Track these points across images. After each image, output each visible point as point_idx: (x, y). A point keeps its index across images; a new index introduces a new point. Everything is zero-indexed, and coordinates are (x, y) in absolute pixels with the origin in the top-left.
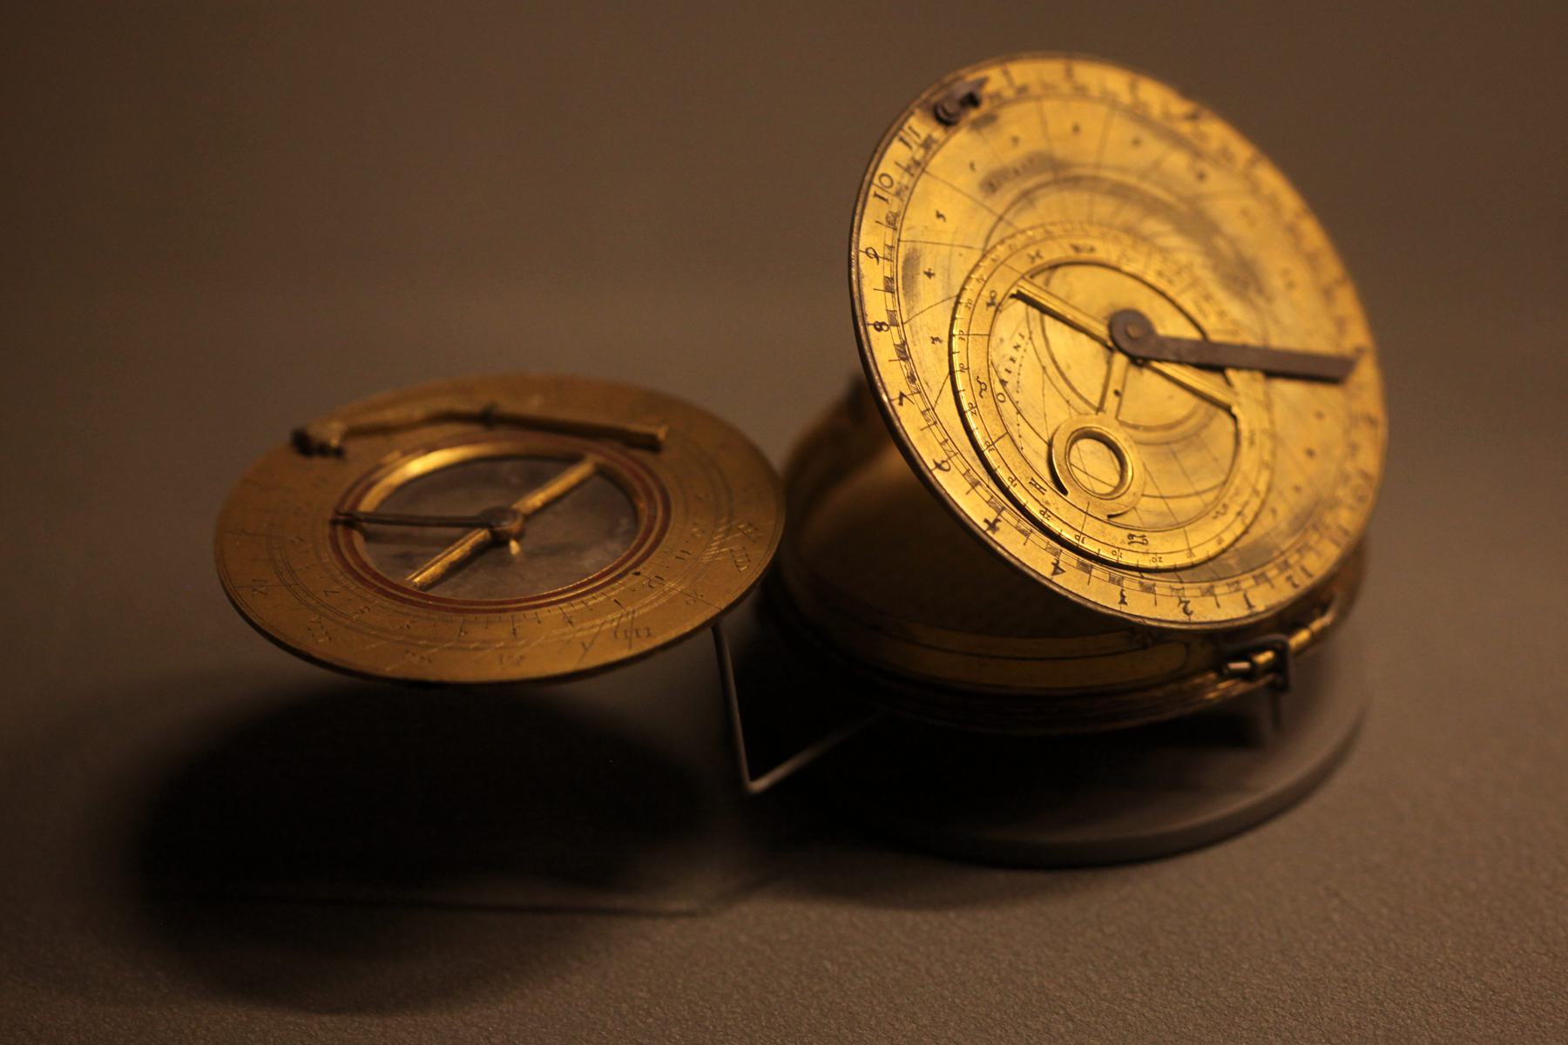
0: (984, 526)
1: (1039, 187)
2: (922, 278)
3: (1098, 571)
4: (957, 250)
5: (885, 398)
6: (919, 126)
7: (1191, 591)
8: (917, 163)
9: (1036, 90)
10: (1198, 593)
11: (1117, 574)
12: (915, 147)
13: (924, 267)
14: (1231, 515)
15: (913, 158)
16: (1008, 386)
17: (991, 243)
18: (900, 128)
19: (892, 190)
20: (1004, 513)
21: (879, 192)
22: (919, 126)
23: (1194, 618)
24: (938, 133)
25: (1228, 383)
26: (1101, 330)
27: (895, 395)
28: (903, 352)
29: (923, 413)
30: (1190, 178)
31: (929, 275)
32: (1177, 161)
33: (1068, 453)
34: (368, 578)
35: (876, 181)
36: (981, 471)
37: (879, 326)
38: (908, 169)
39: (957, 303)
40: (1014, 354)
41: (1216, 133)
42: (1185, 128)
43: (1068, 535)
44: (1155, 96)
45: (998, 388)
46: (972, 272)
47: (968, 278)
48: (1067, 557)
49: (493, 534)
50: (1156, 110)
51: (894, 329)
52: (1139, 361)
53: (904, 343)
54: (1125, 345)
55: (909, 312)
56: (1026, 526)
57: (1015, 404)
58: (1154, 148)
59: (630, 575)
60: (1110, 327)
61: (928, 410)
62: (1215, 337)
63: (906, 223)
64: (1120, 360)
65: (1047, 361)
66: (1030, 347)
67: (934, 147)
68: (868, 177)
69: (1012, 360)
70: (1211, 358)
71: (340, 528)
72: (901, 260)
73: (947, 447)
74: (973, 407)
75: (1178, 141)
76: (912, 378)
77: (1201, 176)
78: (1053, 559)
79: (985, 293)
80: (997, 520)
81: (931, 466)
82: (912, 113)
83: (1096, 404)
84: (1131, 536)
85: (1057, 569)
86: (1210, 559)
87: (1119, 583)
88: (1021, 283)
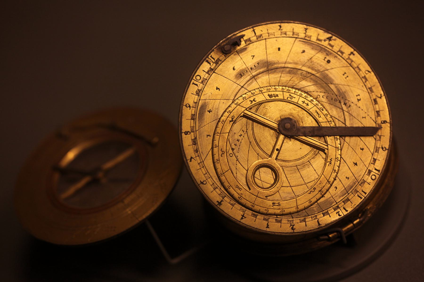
0: (217, 203)
1: (263, 72)
3: (259, 217)
4: (222, 101)
5: (185, 159)
6: (215, 55)
7: (296, 221)
8: (212, 70)
9: (265, 36)
10: (299, 221)
11: (266, 217)
12: (212, 64)
14: (316, 192)
15: (210, 68)
16: (235, 150)
17: (235, 99)
18: (207, 57)
19: (200, 81)
20: (225, 198)
21: (195, 82)
22: (215, 55)
23: (295, 231)
24: (222, 57)
25: (326, 142)
26: (275, 125)
27: (189, 158)
28: (194, 142)
29: (199, 164)
30: (324, 63)
32: (319, 58)
33: (254, 174)
35: (194, 78)
36: (219, 184)
37: (186, 133)
38: (208, 73)
39: (219, 121)
40: (240, 138)
41: (338, 44)
42: (326, 44)
44: (315, 33)
45: (231, 151)
50: (314, 39)
51: (192, 133)
52: (289, 136)
53: (196, 138)
54: (283, 132)
55: (199, 126)
56: (233, 202)
57: (236, 157)
58: (310, 52)
60: (279, 125)
61: (202, 163)
62: (323, 125)
64: (282, 137)
66: (246, 136)
67: (220, 62)
68: (192, 77)
69: (238, 140)
70: (319, 132)
72: (199, 107)
73: (206, 175)
75: (321, 49)
76: (196, 151)
77: (329, 62)
78: (242, 213)
80: (222, 201)
82: (213, 51)
83: (270, 154)
84: (273, 203)
86: (305, 209)
87: (267, 220)
88: (246, 112)
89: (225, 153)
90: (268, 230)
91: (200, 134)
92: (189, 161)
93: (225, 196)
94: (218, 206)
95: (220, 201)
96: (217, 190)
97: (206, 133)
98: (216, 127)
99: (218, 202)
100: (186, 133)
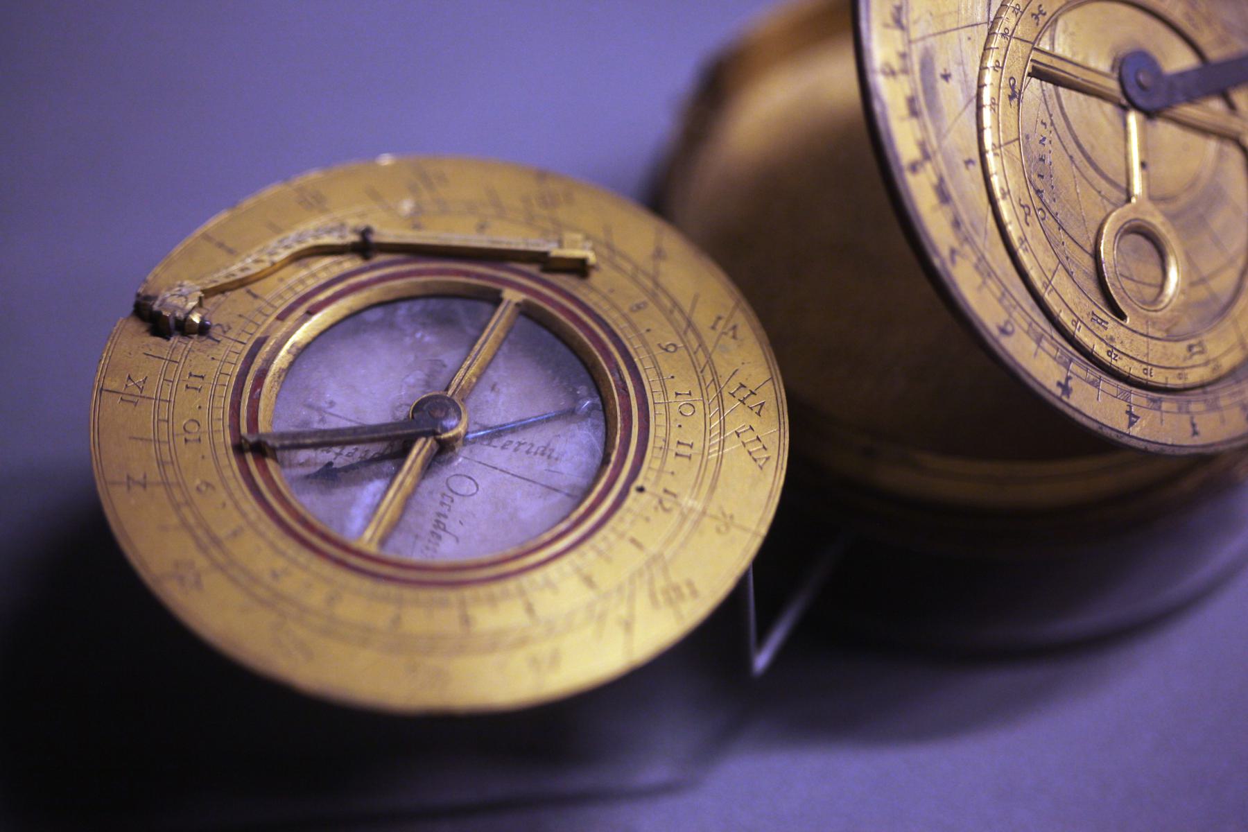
0: (1058, 391)
2: (941, 84)
3: (1168, 404)
13: (939, 70)
20: (1072, 366)
26: (1112, 85)
27: (945, 252)
28: (943, 195)
31: (946, 77)
34: (315, 540)
37: (914, 167)
39: (979, 107)
43: (1136, 371)
46: (983, 58)
47: (982, 68)
48: (1138, 398)
49: (439, 442)
54: (1140, 101)
56: (1093, 374)
59: (633, 493)
60: (1121, 81)
63: (913, 15)
64: (1133, 118)
65: (1072, 148)
71: (249, 458)
72: (917, 68)
74: (1023, 240)
79: (1004, 82)
80: (1068, 378)
81: (996, 332)
84: (1190, 348)
85: (1132, 418)
89: (1032, 212)
90: (1198, 441)
91: (948, 162)
92: (949, 265)
93: (1071, 360)
94: (1064, 398)
95: (1063, 381)
96: (1045, 344)
97: (959, 160)
98: (980, 130)
99: (1059, 384)
100: (914, 167)
